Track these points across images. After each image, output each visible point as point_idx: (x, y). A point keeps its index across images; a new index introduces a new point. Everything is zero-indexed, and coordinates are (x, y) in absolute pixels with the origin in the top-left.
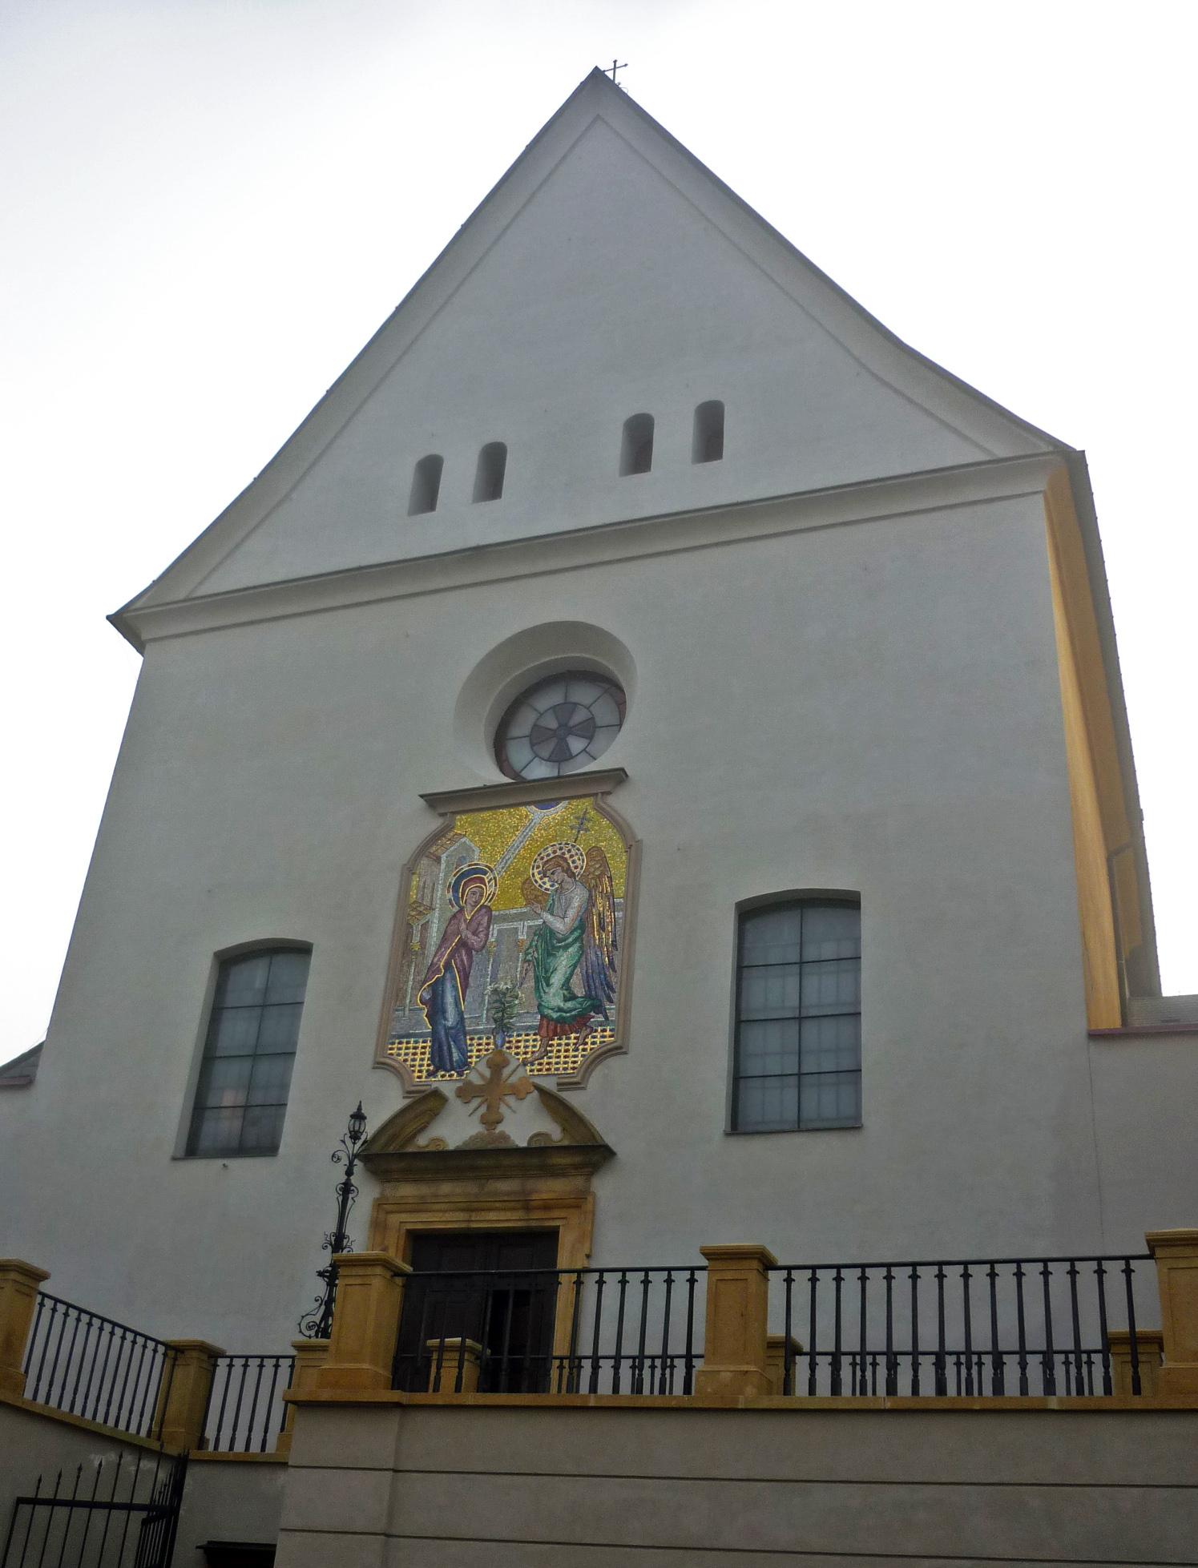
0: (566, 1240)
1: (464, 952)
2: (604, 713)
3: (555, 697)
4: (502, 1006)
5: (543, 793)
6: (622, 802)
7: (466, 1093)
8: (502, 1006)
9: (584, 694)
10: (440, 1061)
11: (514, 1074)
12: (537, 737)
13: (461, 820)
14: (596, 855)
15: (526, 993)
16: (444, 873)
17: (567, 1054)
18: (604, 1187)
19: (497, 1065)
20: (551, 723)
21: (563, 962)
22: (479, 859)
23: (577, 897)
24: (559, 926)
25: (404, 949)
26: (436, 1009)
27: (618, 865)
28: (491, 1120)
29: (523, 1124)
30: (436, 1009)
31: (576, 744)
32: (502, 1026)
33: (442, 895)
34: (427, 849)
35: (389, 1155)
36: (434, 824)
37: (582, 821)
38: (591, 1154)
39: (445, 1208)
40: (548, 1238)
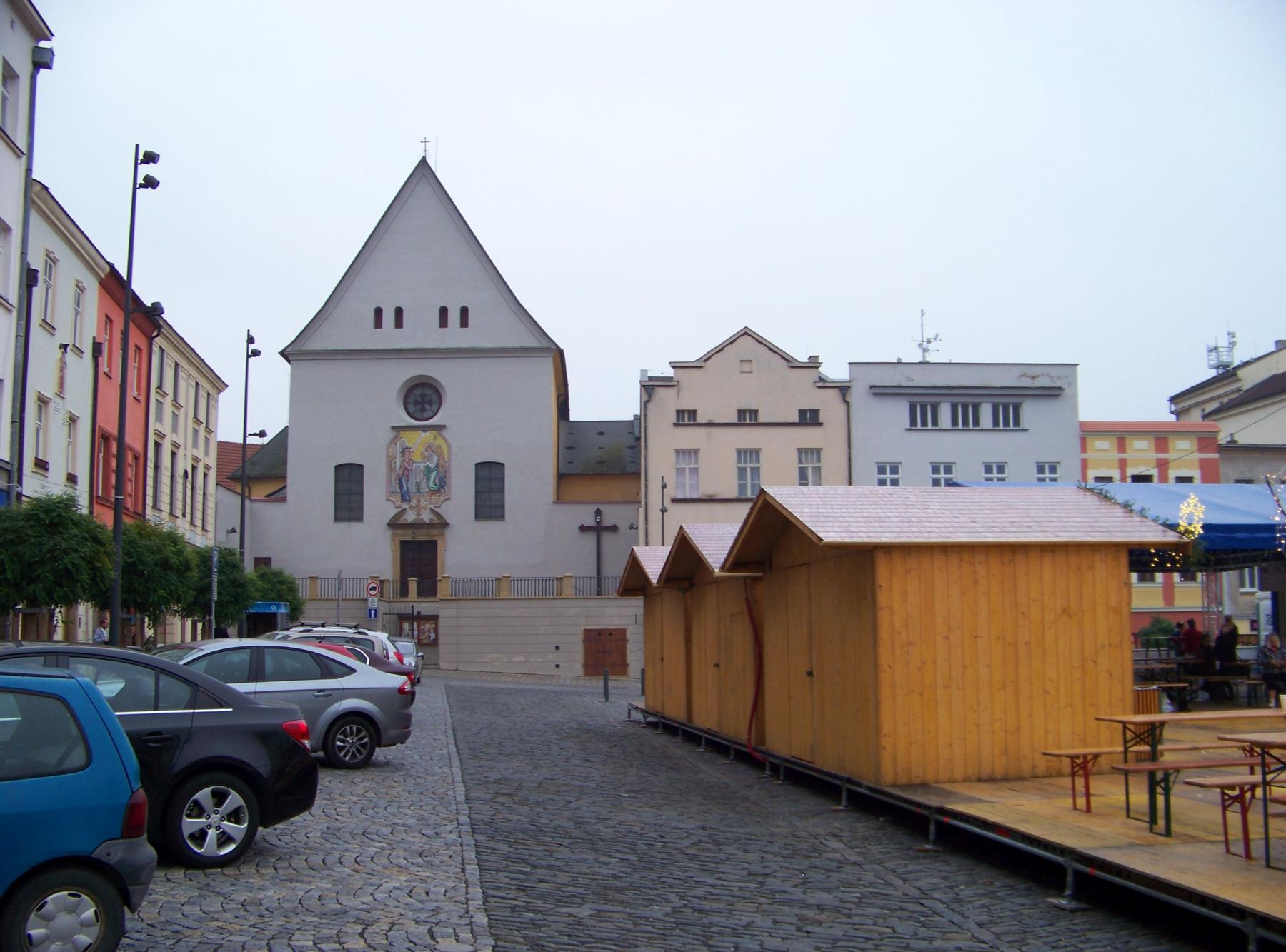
0: (439, 543)
1: (406, 472)
2: (435, 398)
3: (422, 397)
4: (418, 485)
5: (425, 429)
6: (445, 433)
7: (411, 508)
8: (418, 485)
9: (428, 391)
10: (404, 500)
11: (423, 503)
12: (416, 403)
13: (402, 434)
14: (439, 447)
15: (424, 483)
16: (399, 449)
17: (435, 497)
18: (448, 532)
19: (419, 501)
20: (419, 399)
21: (433, 475)
22: (407, 444)
23: (435, 459)
24: (431, 466)
25: (391, 468)
26: (401, 486)
27: (445, 451)
28: (419, 515)
29: (426, 517)
30: (401, 486)
31: (427, 407)
32: (419, 491)
33: (398, 454)
34: (393, 441)
35: (394, 525)
36: (394, 434)
37: (435, 438)
38: (444, 525)
39: (408, 536)
40: (435, 542)
